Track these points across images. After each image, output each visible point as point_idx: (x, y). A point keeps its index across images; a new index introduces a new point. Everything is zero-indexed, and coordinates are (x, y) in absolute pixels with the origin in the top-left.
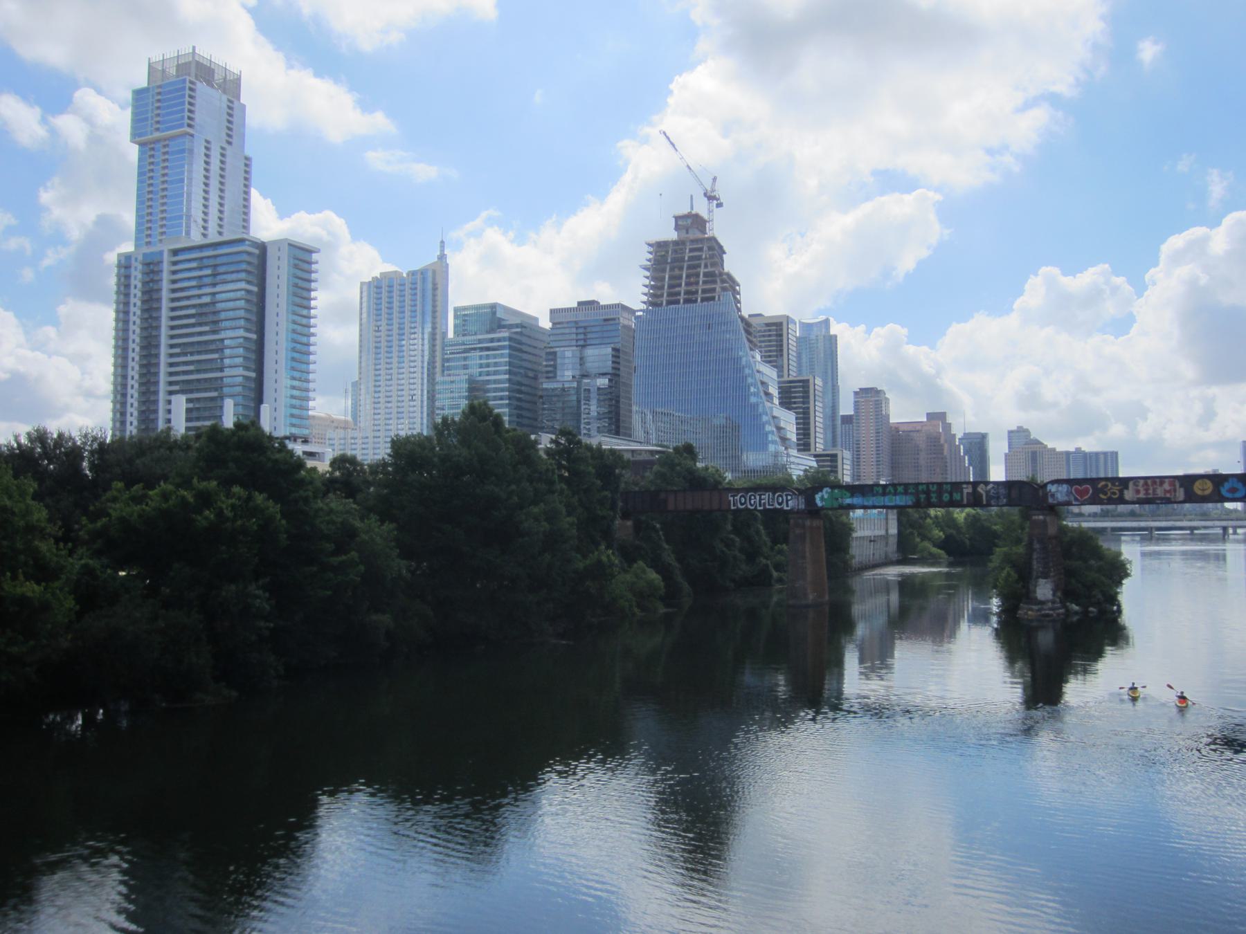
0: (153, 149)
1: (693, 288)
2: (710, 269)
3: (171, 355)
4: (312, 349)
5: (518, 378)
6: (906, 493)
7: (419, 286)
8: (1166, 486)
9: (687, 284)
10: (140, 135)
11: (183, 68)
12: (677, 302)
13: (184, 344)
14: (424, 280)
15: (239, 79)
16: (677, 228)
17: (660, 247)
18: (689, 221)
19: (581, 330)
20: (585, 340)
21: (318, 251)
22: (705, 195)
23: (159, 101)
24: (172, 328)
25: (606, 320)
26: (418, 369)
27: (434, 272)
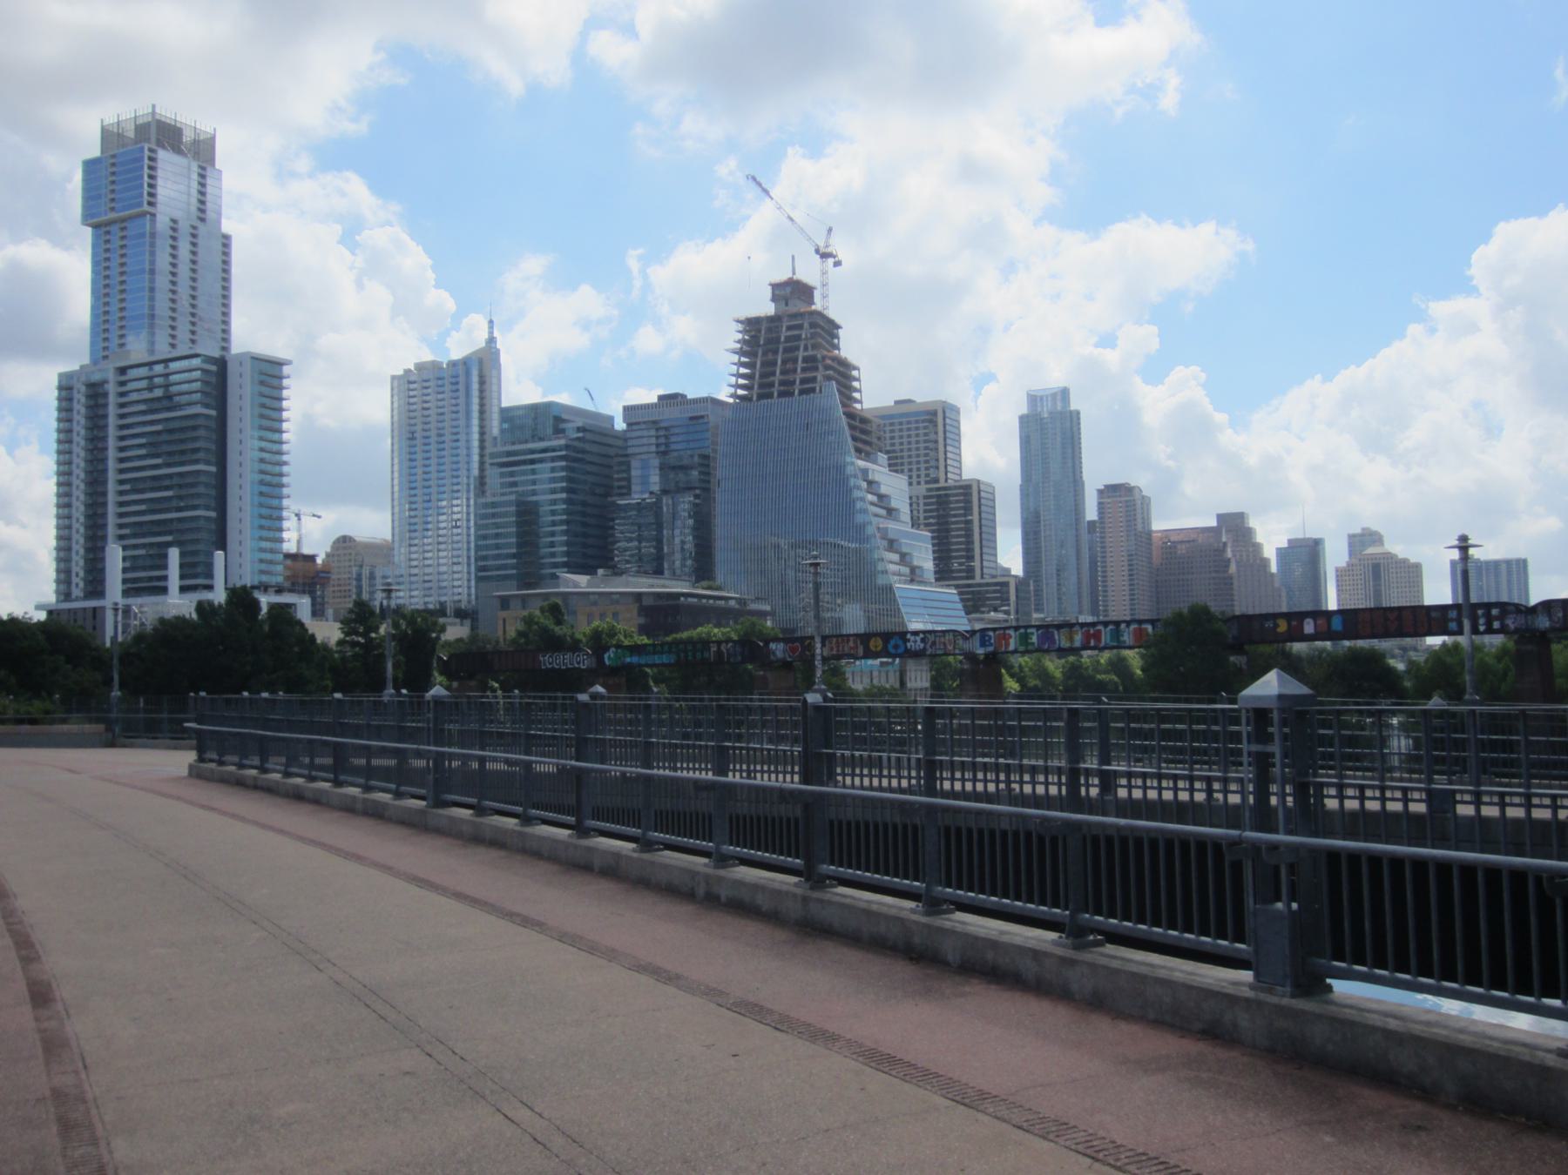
0: (108, 233)
1: (791, 377)
2: (810, 353)
3: (121, 493)
4: (285, 480)
5: (580, 497)
6: (670, 652)
7: (462, 379)
8: (851, 644)
9: (782, 373)
10: (93, 216)
11: (142, 130)
12: (770, 396)
13: (136, 479)
14: (468, 374)
15: (213, 138)
16: (774, 299)
17: (752, 325)
18: (788, 290)
19: (662, 433)
20: (666, 445)
21: (288, 363)
22: (817, 251)
23: (113, 174)
24: (121, 460)
25: (691, 418)
26: (463, 488)
27: (481, 362)
